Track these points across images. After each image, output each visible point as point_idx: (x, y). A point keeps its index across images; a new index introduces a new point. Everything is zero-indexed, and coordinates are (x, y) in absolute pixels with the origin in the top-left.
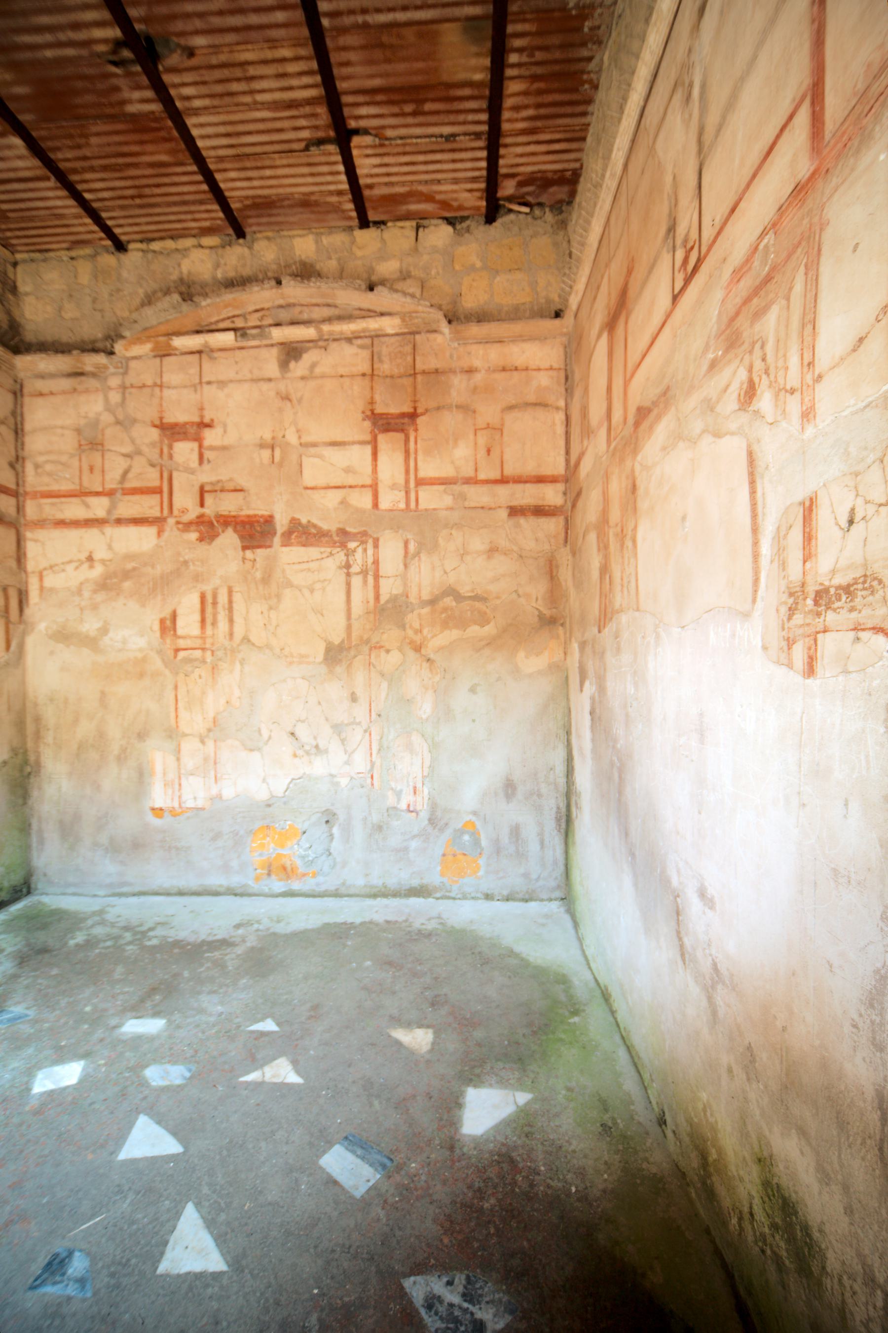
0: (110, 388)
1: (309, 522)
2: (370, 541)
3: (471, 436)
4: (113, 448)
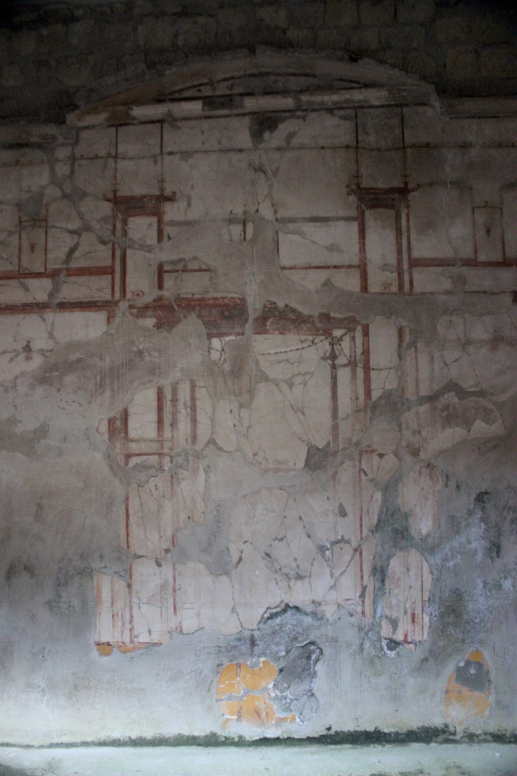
0: (57, 160)
1: (286, 306)
2: (359, 328)
3: (469, 214)
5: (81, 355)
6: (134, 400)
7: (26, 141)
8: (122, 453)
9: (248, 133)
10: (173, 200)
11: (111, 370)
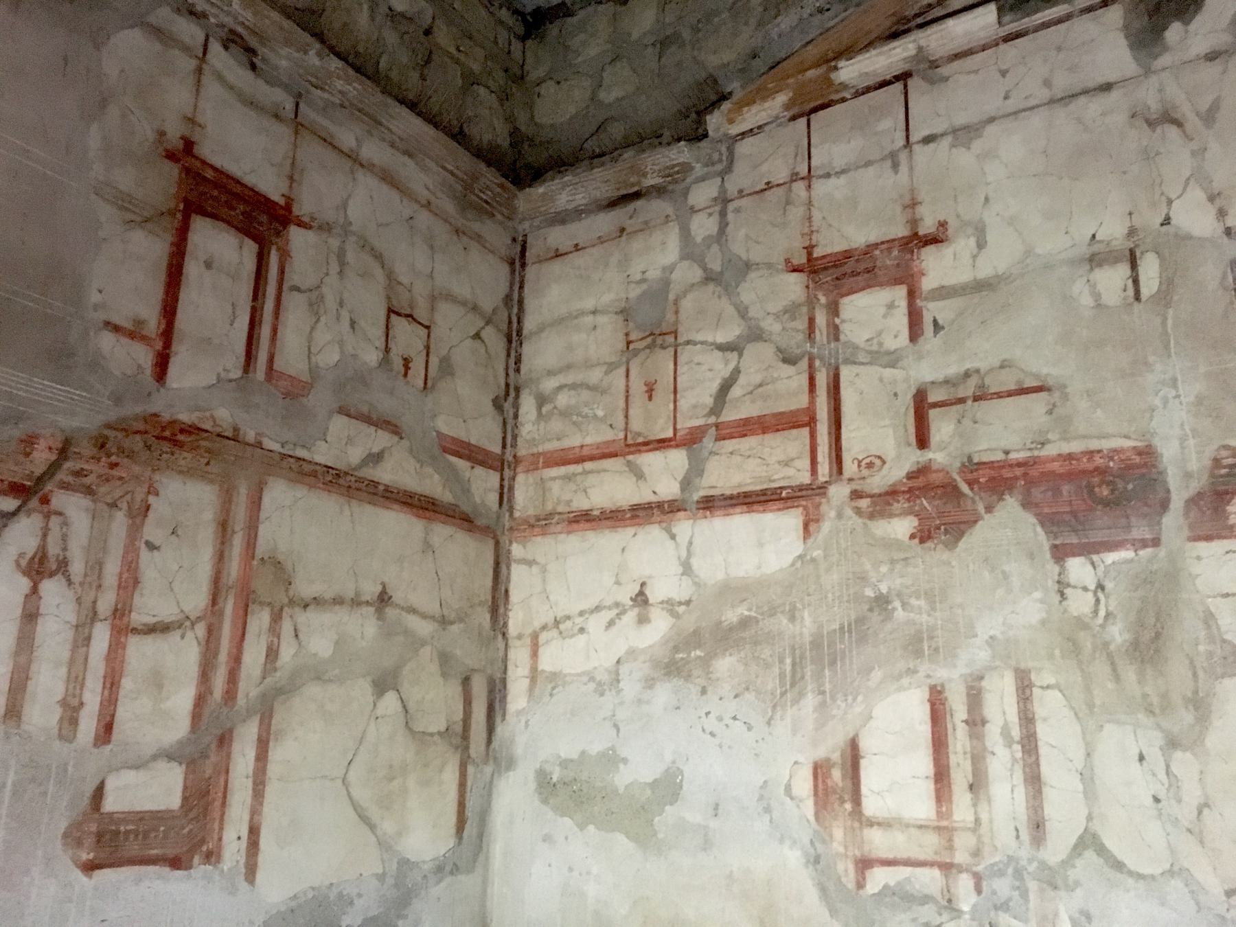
0: (693, 210)
4: (699, 337)
5: (750, 610)
6: (871, 717)
7: (636, 189)
8: (850, 854)
9: (1122, 42)
10: (942, 241)
11: (816, 644)
